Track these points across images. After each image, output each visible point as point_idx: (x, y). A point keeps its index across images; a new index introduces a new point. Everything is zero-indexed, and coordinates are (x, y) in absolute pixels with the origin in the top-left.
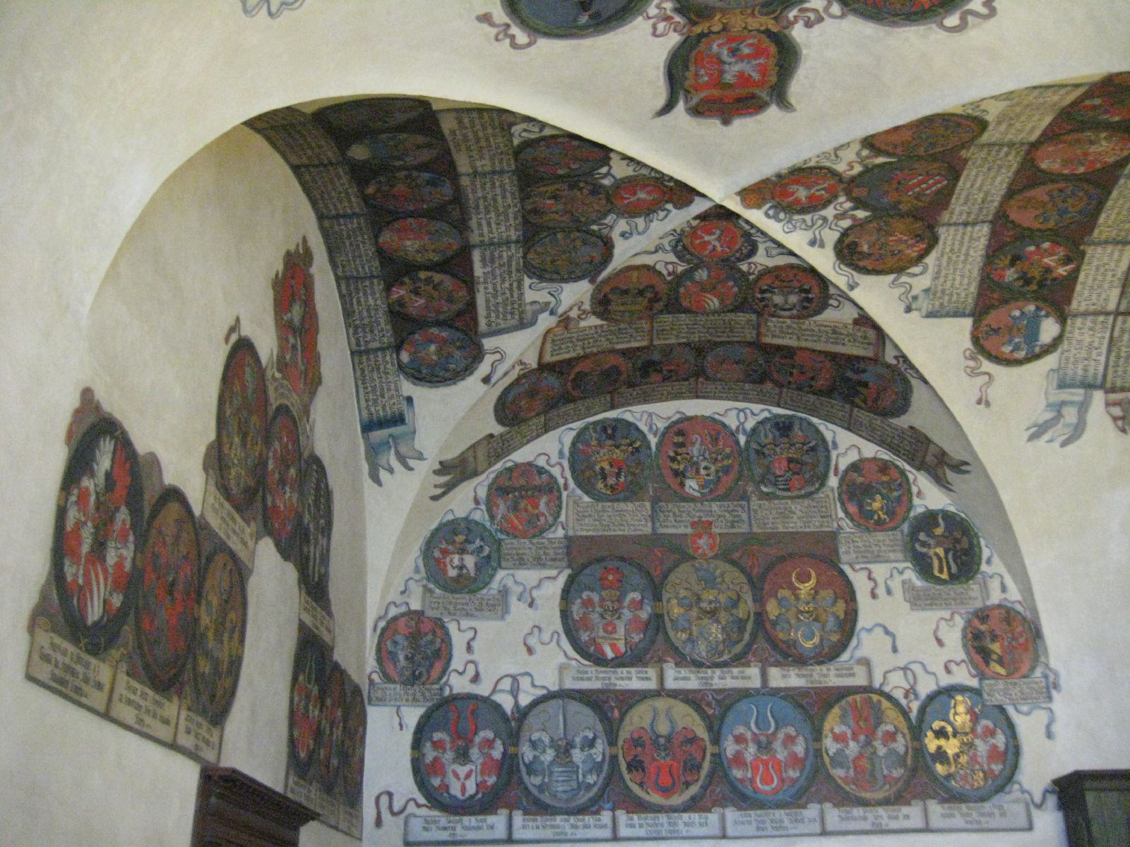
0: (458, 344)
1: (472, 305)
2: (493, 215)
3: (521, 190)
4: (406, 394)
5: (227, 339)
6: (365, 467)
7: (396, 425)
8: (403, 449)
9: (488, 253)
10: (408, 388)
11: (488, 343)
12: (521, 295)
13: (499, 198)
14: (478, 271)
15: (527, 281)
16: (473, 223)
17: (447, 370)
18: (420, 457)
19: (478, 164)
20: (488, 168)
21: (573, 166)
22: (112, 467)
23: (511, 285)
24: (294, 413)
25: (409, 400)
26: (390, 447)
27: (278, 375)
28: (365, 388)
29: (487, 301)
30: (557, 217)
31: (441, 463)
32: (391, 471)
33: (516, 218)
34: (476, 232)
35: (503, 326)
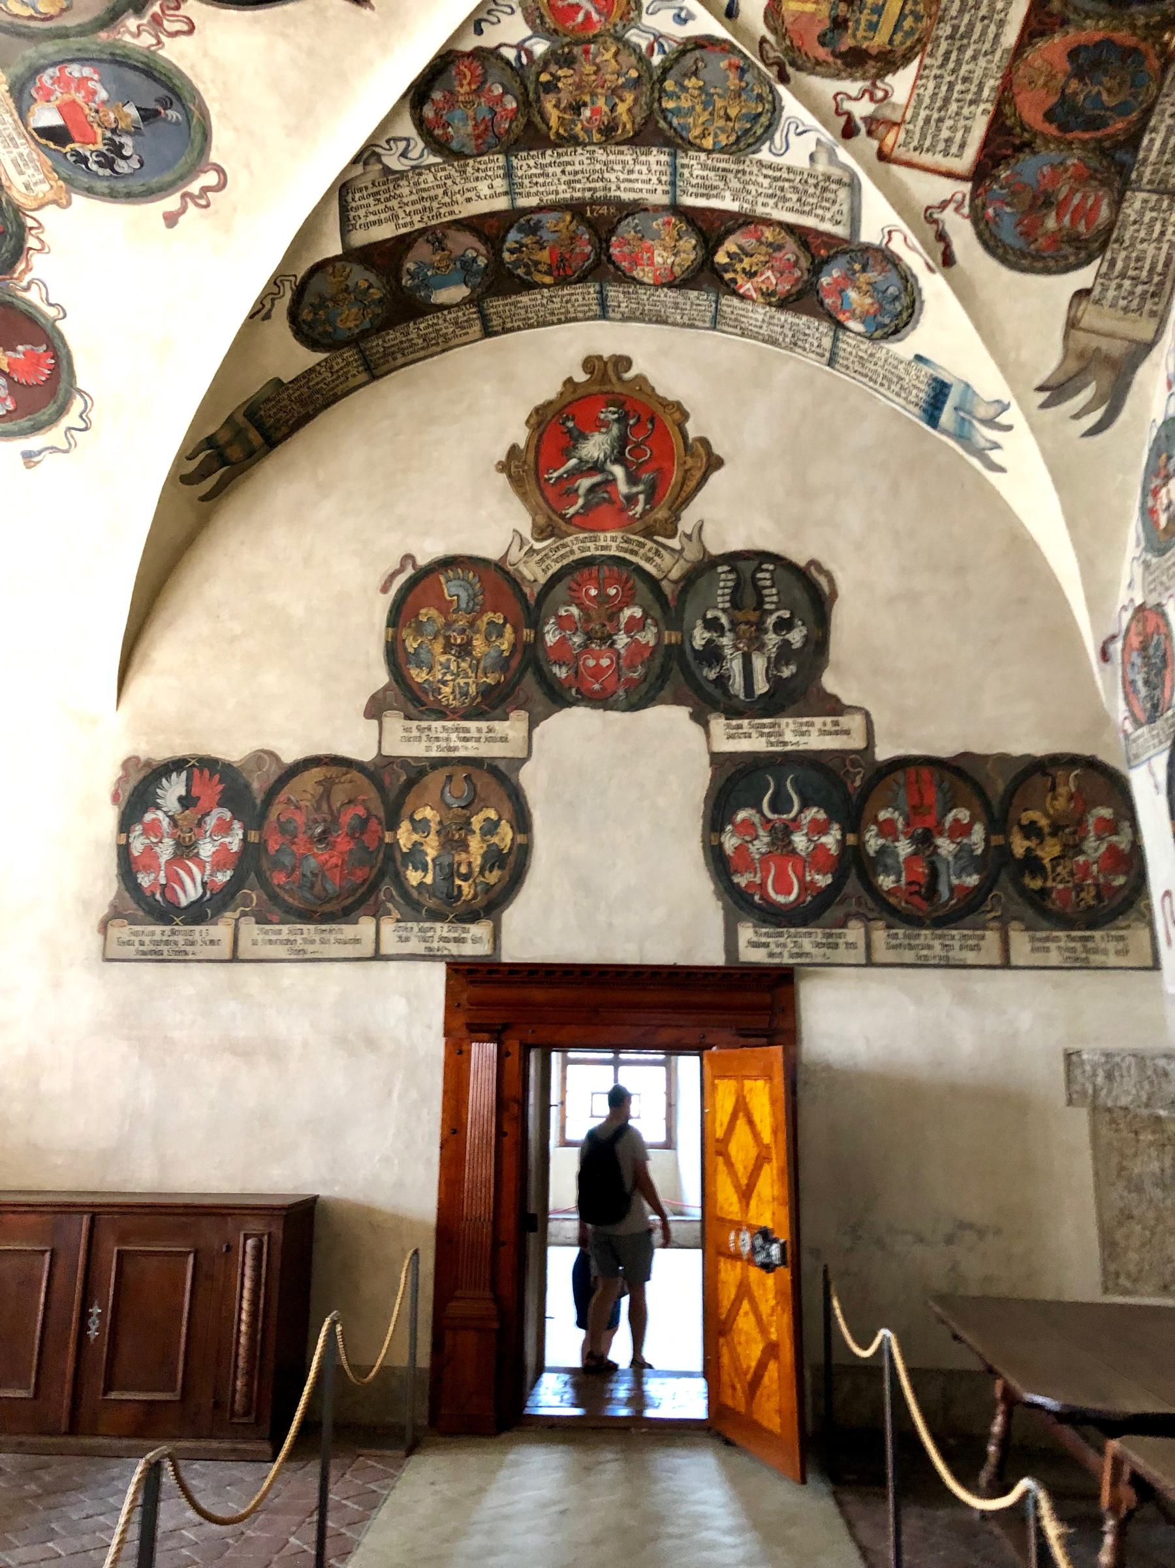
0: (857, 267)
1: (790, 229)
2: (612, 176)
3: (555, 146)
4: (911, 357)
5: (385, 589)
6: (975, 462)
7: (946, 396)
8: (982, 412)
9: (691, 190)
10: (903, 348)
11: (870, 234)
12: (790, 170)
13: (569, 168)
14: (727, 203)
15: (764, 155)
16: (626, 196)
17: (896, 298)
18: (1006, 407)
19: (487, 192)
20: (500, 184)
21: (498, 90)
22: (188, 791)
23: (766, 176)
24: (613, 552)
25: (919, 358)
26: (970, 423)
27: (538, 546)
28: (882, 385)
29: (791, 210)
30: (622, 108)
31: (1041, 389)
32: (996, 446)
33: (621, 153)
34: (644, 195)
35: (845, 208)
